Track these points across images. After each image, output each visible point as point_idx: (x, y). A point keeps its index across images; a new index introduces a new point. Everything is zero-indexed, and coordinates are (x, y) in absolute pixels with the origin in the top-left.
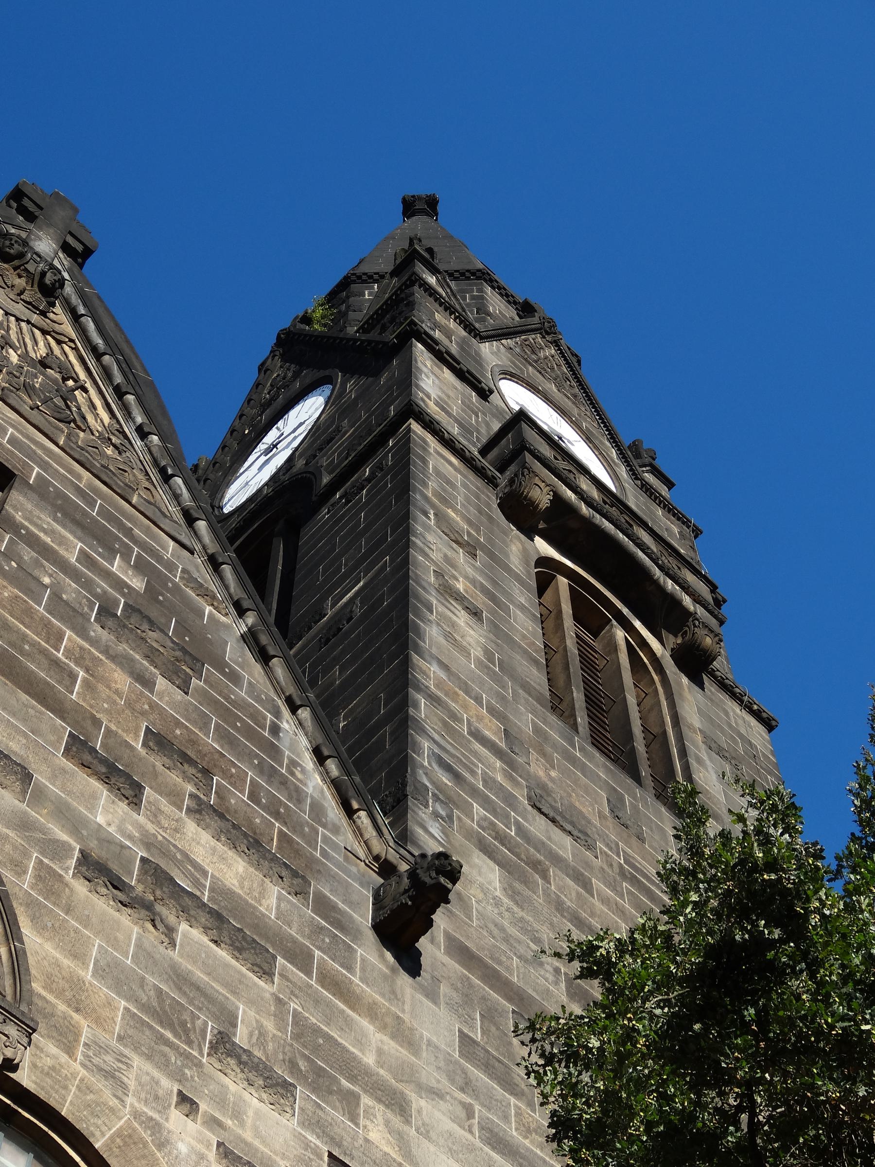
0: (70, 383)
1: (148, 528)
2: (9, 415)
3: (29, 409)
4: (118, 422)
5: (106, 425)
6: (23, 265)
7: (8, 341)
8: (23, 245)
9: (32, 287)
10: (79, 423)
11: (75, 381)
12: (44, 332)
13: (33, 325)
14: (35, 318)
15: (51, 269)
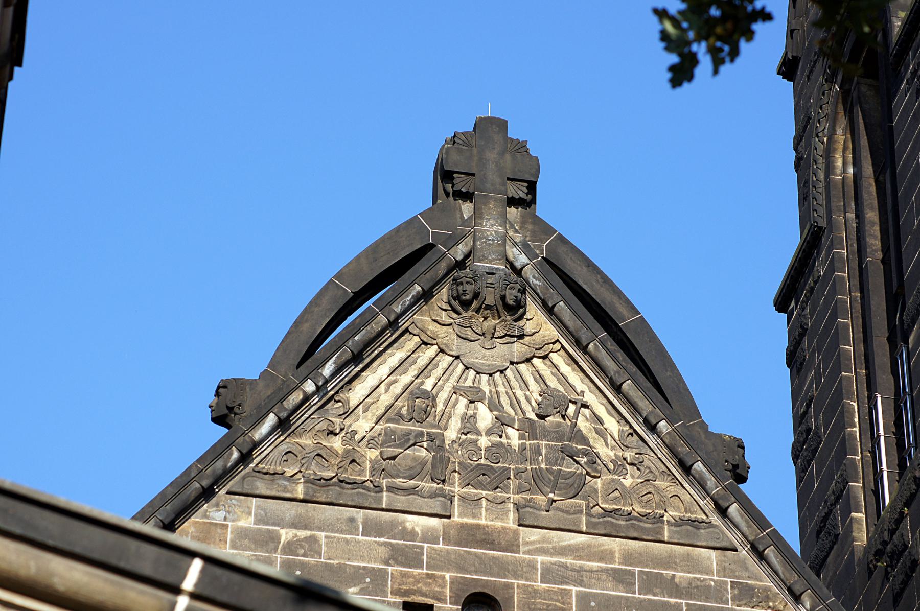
0: (572, 408)
1: (688, 556)
2: (533, 538)
3: (545, 513)
4: (627, 421)
5: (617, 438)
6: (483, 303)
7: (504, 422)
8: (474, 281)
9: (500, 317)
10: (593, 474)
11: (574, 403)
12: (528, 360)
13: (517, 363)
14: (518, 349)
15: (508, 285)
